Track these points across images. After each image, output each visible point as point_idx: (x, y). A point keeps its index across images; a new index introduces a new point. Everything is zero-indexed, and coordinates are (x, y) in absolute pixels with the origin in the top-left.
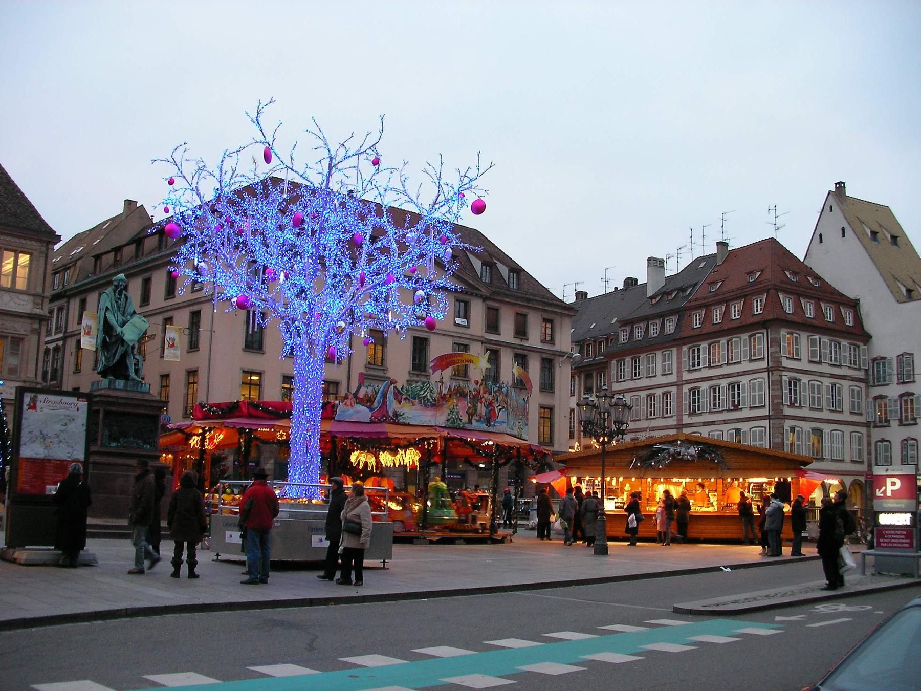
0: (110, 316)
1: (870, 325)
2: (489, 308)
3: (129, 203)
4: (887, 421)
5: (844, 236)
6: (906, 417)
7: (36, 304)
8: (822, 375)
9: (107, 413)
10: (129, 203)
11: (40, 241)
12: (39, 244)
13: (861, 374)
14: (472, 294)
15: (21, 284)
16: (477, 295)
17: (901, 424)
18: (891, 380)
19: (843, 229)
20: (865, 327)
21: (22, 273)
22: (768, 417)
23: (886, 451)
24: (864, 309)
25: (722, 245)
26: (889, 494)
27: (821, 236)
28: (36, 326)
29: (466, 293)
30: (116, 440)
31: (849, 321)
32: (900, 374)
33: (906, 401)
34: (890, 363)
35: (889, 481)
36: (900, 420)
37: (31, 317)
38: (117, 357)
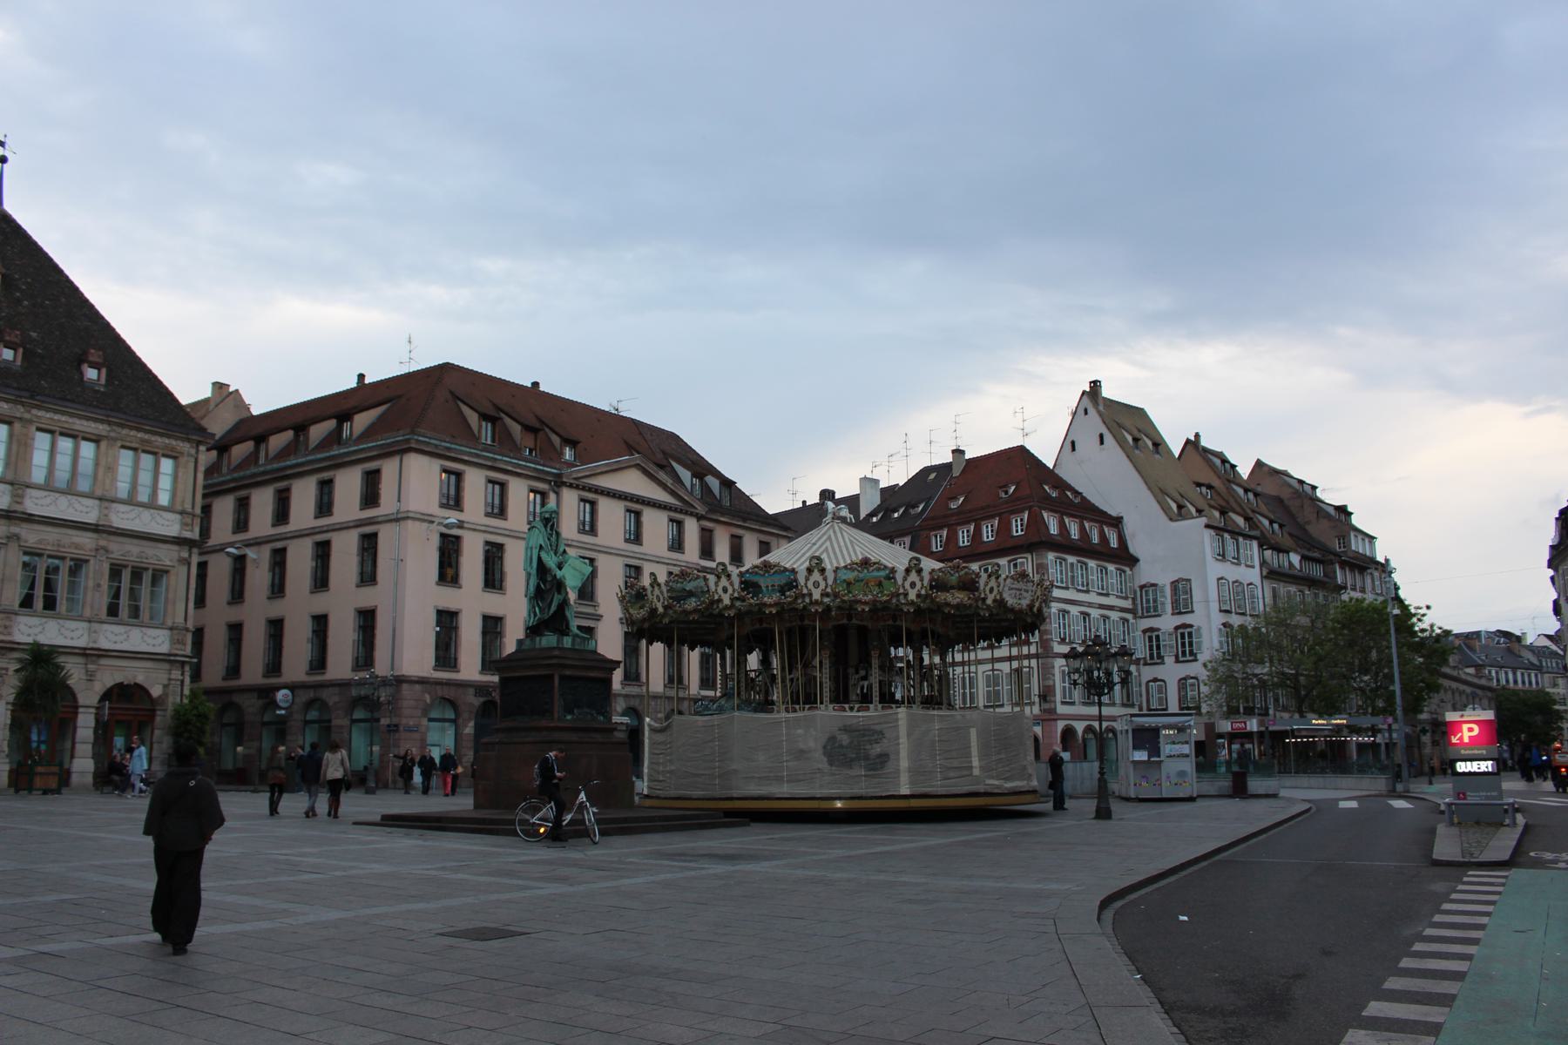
0: (543, 555)
1: (1135, 548)
2: (703, 530)
3: (219, 387)
4: (1160, 657)
5: (1102, 443)
6: (1184, 653)
7: (184, 525)
8: (1111, 608)
9: (562, 678)
10: (219, 387)
11: (189, 440)
12: (187, 445)
13: (1127, 604)
14: (686, 513)
15: (164, 499)
16: (691, 514)
17: (1177, 661)
18: (1164, 611)
19: (1101, 436)
20: (1131, 550)
21: (165, 483)
22: (1037, 656)
23: (1160, 692)
24: (1129, 527)
25: (958, 452)
26: (1466, 740)
27: (1073, 443)
28: (185, 554)
29: (681, 512)
30: (571, 712)
31: (1114, 543)
32: (1175, 603)
33: (1183, 635)
34: (1162, 591)
35: (1465, 727)
36: (1177, 657)
37: (179, 541)
38: (553, 608)
